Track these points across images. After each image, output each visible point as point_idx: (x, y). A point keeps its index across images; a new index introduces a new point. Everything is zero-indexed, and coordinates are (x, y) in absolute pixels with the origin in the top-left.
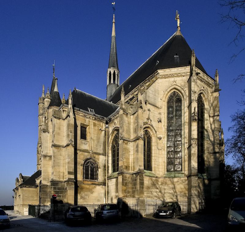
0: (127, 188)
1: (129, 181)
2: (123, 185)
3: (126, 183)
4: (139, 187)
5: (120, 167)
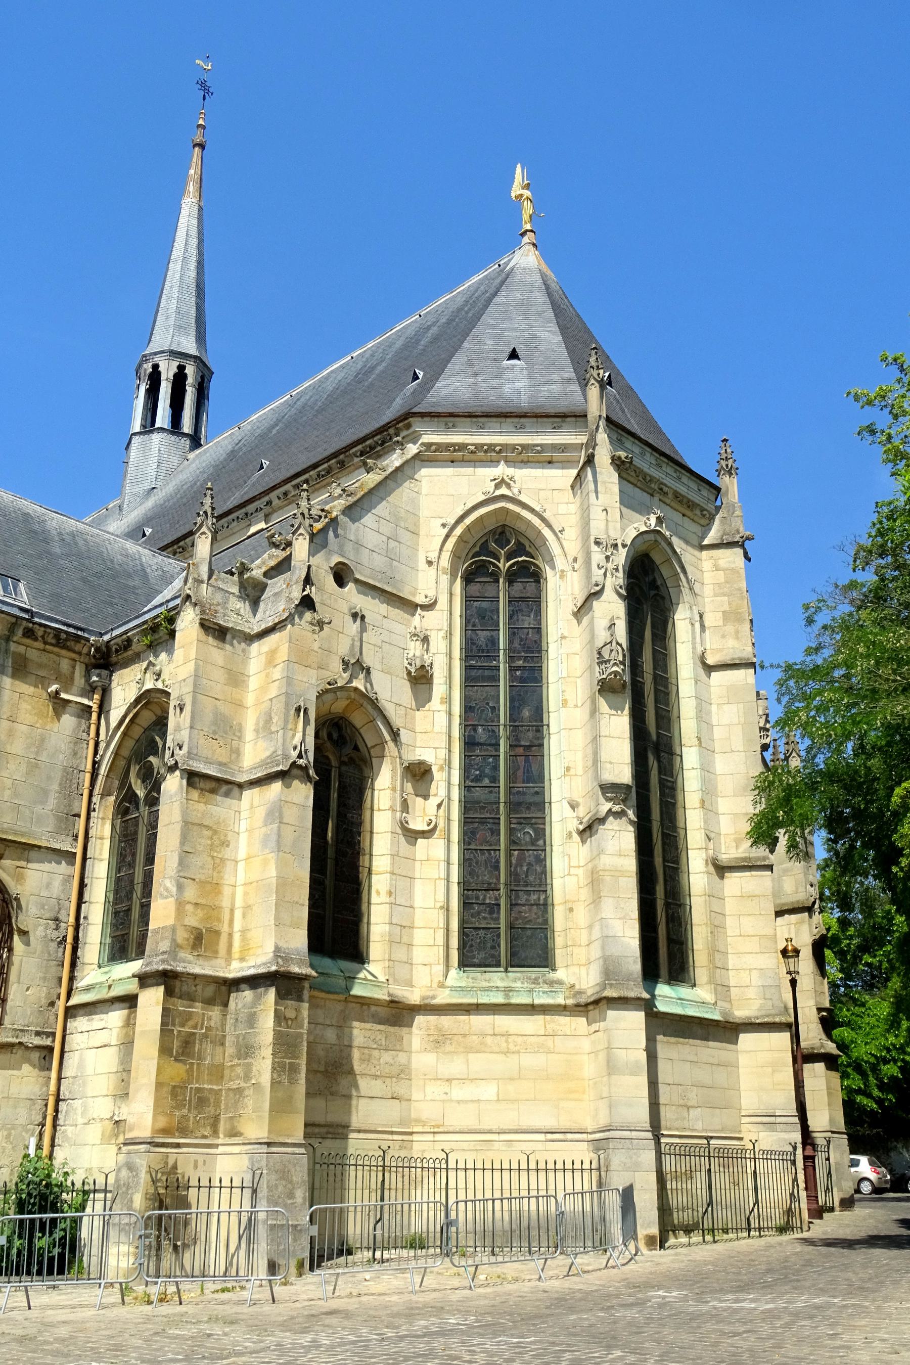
0: (190, 1071)
1: (209, 1029)
2: (165, 1050)
3: (188, 1042)
4: (274, 1069)
5: (156, 932)
